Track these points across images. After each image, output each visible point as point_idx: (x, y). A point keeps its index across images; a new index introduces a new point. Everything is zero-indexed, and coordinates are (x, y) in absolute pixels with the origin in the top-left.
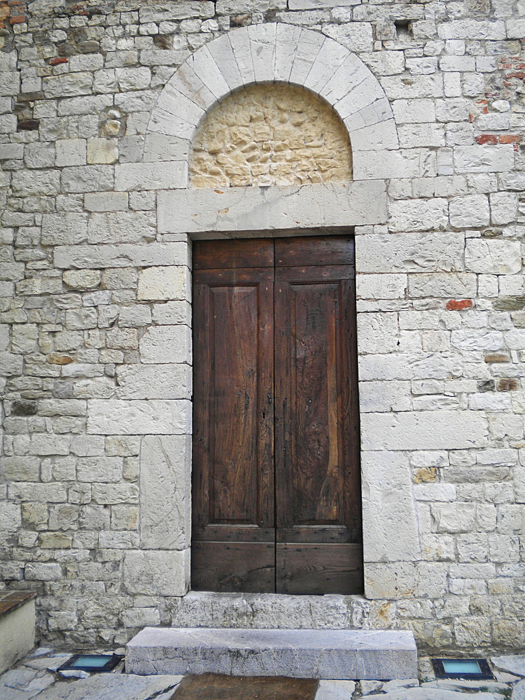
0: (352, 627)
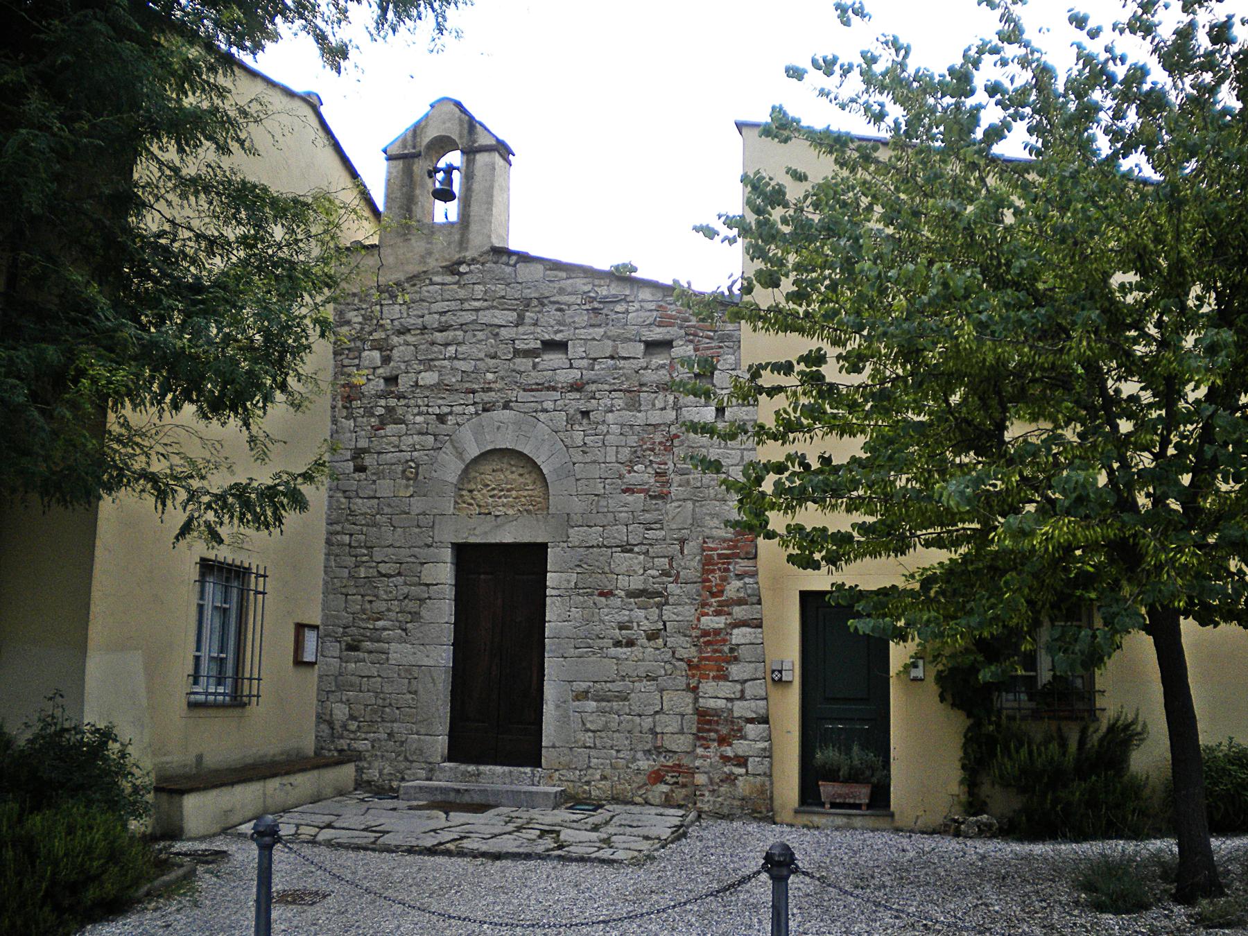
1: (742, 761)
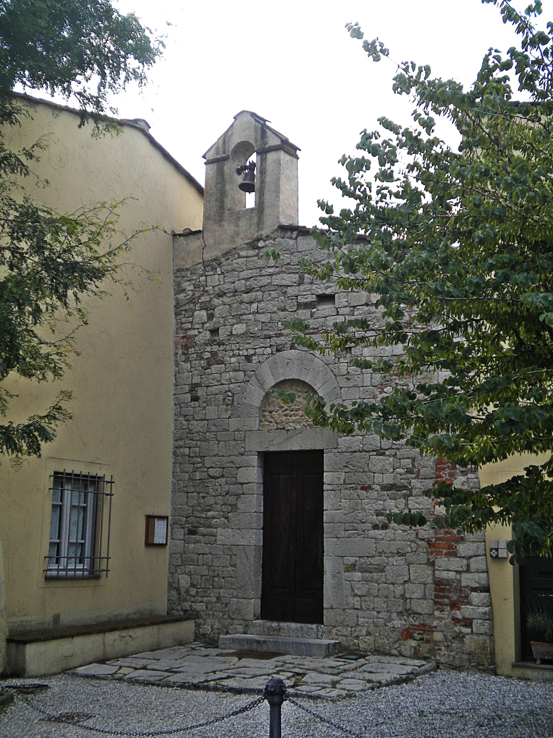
0: (318, 638)
1: (468, 623)
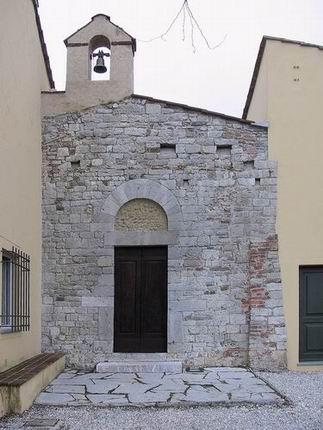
1: (274, 345)
